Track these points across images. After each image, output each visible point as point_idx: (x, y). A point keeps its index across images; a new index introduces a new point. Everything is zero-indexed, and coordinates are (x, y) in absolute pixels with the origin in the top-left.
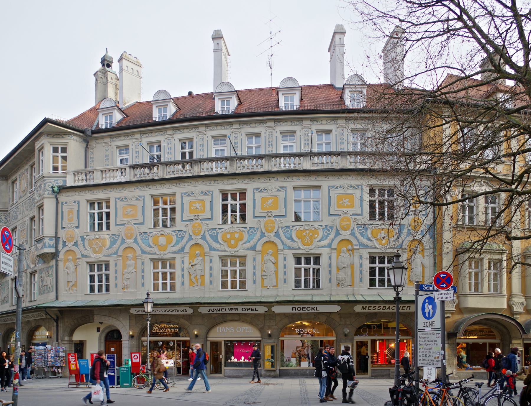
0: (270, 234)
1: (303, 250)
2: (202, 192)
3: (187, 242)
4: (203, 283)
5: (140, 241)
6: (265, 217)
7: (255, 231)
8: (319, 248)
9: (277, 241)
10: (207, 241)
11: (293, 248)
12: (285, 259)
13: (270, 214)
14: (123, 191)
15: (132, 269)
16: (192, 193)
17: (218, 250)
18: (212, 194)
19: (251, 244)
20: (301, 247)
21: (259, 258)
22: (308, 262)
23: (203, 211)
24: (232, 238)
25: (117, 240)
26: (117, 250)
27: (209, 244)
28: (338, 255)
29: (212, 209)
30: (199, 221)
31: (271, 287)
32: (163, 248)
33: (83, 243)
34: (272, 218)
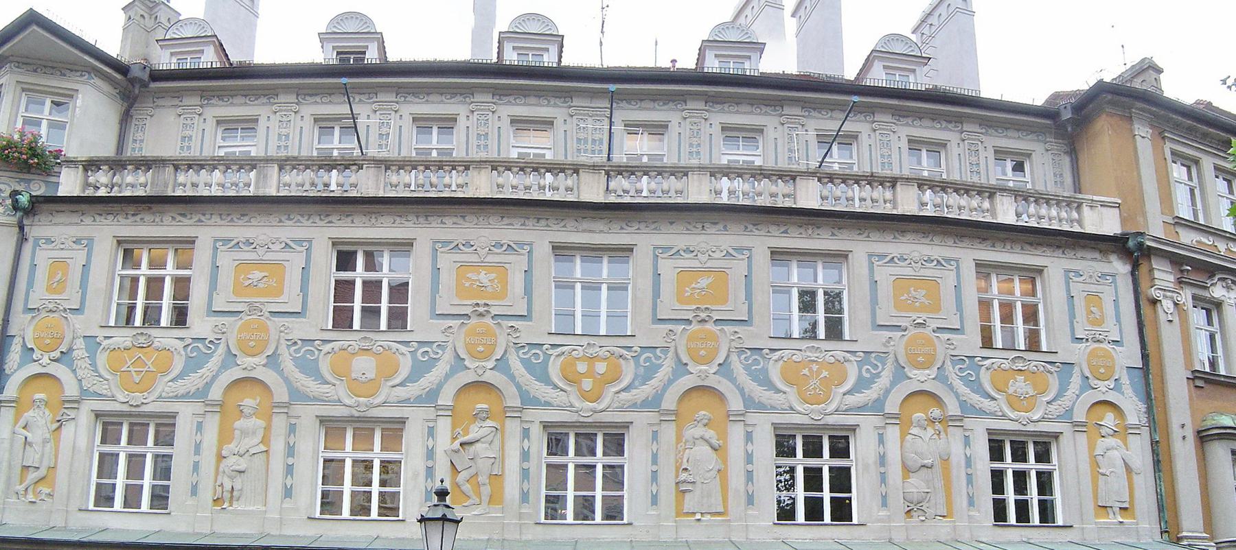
1: (802, 415)
3: (447, 377)
4: (496, 498)
5: (288, 364)
6: (688, 322)
8: (848, 411)
9: (724, 386)
11: (773, 408)
12: (749, 437)
14: (240, 222)
15: (252, 443)
17: (548, 404)
19: (646, 390)
22: (813, 449)
23: (502, 295)
24: (590, 373)
25: (210, 356)
26: (208, 385)
27: (518, 386)
28: (904, 434)
29: (528, 291)
31: (709, 517)
32: (367, 387)
33: (92, 357)
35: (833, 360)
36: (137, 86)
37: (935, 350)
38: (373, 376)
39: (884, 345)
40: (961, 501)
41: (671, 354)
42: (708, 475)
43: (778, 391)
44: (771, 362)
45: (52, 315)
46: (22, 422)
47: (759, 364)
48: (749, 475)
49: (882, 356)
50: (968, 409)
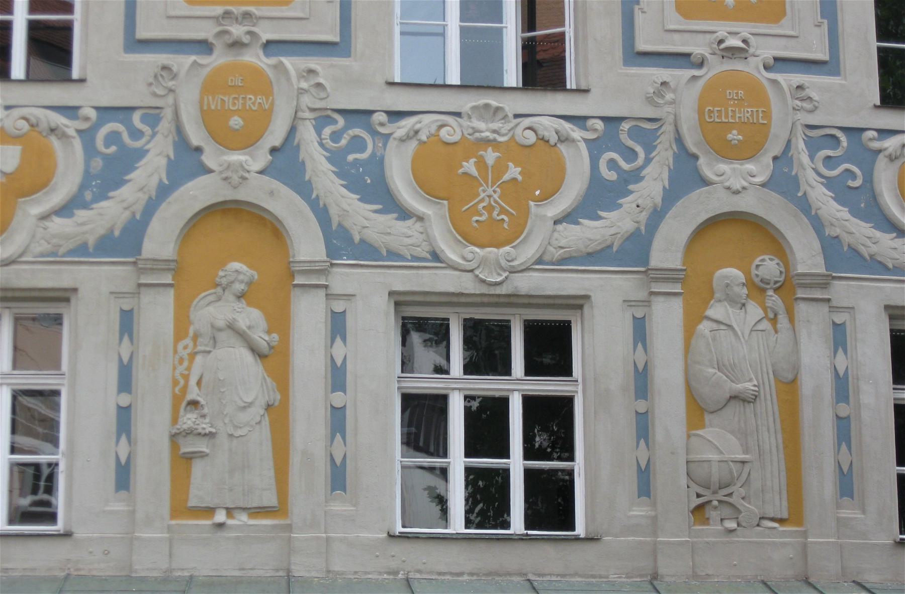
0: (236, 157)
1: (460, 271)
6: (204, 46)
7: (136, 134)
9: (282, 202)
12: (338, 326)
13: (238, 31)
19: (110, 213)
20: (452, 255)
21: (157, 313)
31: (244, 518)
34: (254, 57)
35: (531, 137)
37: (767, 114)
39: (650, 101)
40: (821, 484)
41: (166, 125)
42: (243, 417)
43: (405, 214)
44: (392, 144)
47: (363, 149)
48: (338, 420)
49: (647, 132)
50: (842, 258)
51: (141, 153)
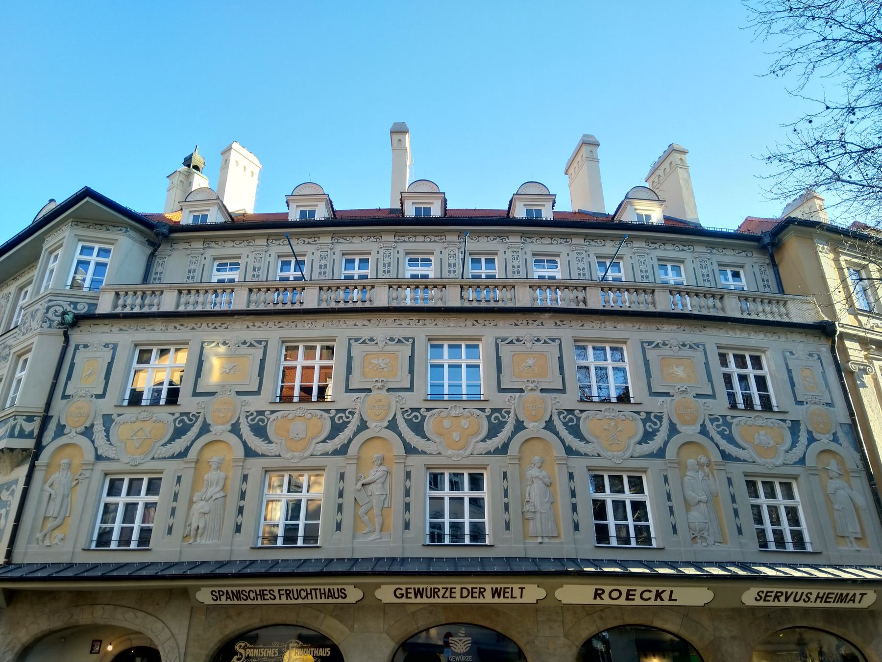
2: (392, 339)
7: (504, 417)
10: (399, 434)
16: (372, 340)
17: (423, 452)
18: (413, 344)
25: (192, 425)
30: (384, 392)
33: (107, 431)
36: (161, 237)
38: (303, 436)
45: (82, 399)
46: (49, 482)
51: (506, 422)
